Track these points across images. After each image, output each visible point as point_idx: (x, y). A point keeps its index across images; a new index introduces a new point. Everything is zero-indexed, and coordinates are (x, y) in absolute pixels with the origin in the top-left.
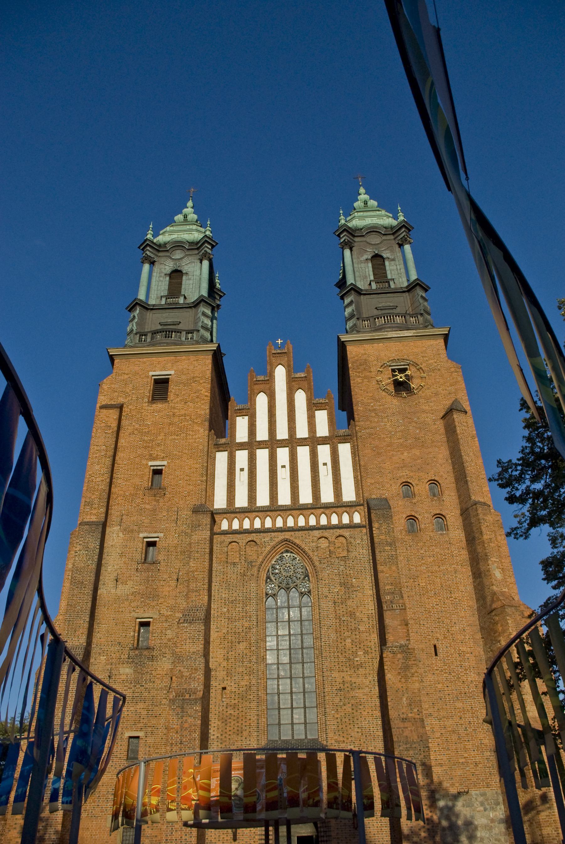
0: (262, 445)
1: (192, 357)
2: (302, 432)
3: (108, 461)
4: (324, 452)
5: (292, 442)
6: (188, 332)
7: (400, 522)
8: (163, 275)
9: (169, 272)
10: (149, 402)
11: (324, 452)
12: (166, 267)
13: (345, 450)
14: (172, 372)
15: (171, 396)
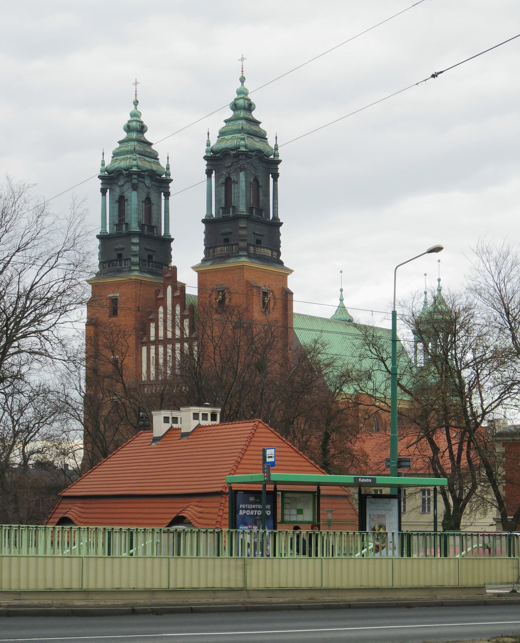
6: (126, 260)
8: (115, 201)
9: (117, 200)
10: (109, 316)
12: (116, 193)
14: (118, 295)
15: (119, 313)
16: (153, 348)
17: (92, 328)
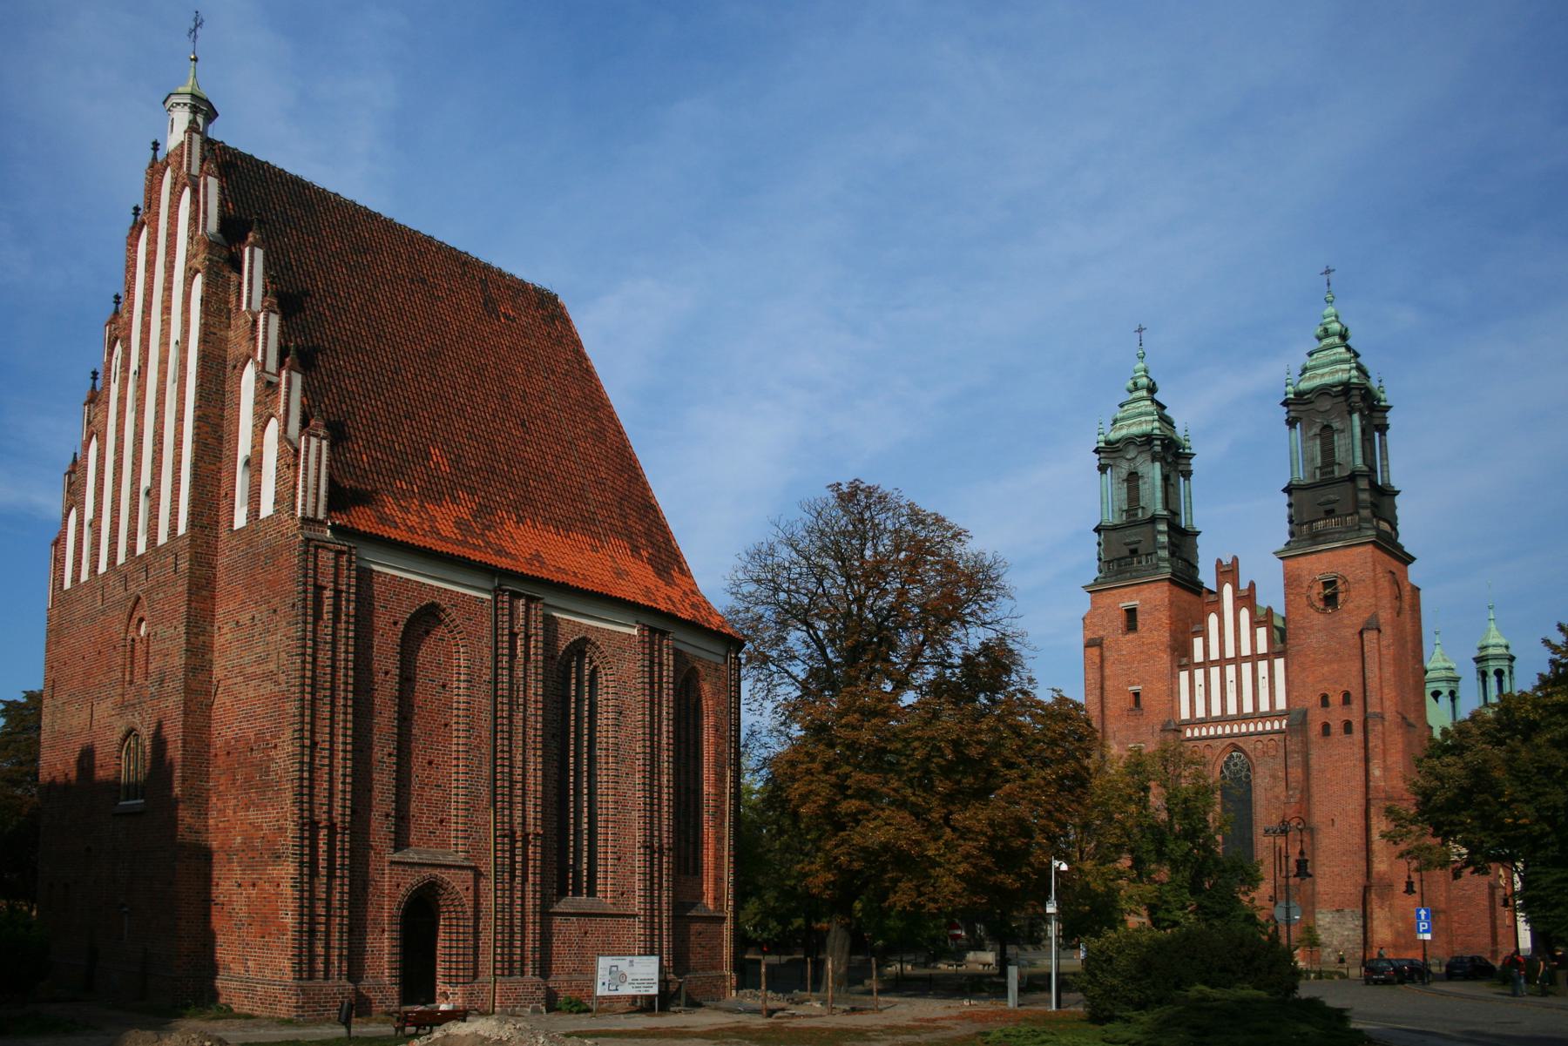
0: (1214, 663)
1: (1153, 586)
2: (1246, 650)
3: (1098, 692)
4: (1263, 666)
5: (1238, 660)
7: (1315, 729)
11: (1263, 666)
13: (1279, 664)
16: (1199, 673)
17: (1095, 651)
